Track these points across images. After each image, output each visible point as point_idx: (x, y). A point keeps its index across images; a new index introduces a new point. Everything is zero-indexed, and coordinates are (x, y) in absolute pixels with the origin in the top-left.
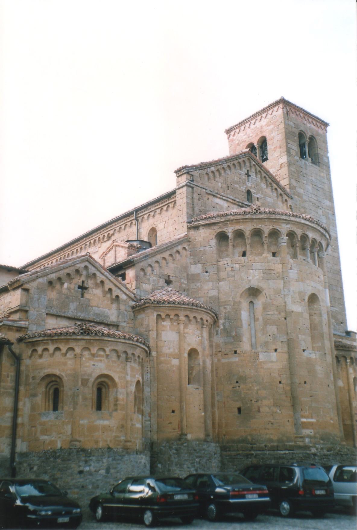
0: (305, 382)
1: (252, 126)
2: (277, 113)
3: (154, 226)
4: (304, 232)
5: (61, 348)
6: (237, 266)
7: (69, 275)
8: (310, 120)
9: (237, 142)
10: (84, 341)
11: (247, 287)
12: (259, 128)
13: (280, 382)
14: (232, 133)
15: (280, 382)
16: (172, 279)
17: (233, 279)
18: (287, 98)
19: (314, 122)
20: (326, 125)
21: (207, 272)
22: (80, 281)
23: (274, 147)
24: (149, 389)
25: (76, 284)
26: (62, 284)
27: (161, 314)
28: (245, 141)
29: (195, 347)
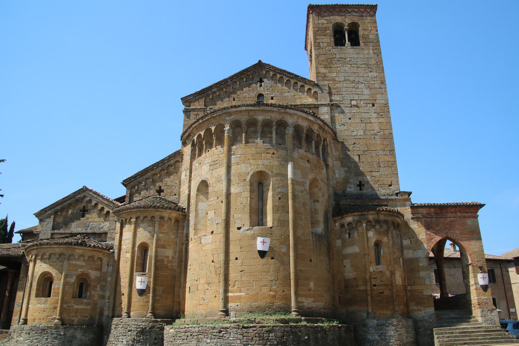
0: (237, 259)
4: (251, 118)
7: (70, 204)
8: (349, 10)
10: (35, 250)
13: (213, 261)
15: (213, 261)
16: (162, 188)
18: (312, 4)
19: (356, 10)
22: (81, 206)
24: (111, 278)
25: (78, 209)
26: (67, 212)
29: (145, 241)
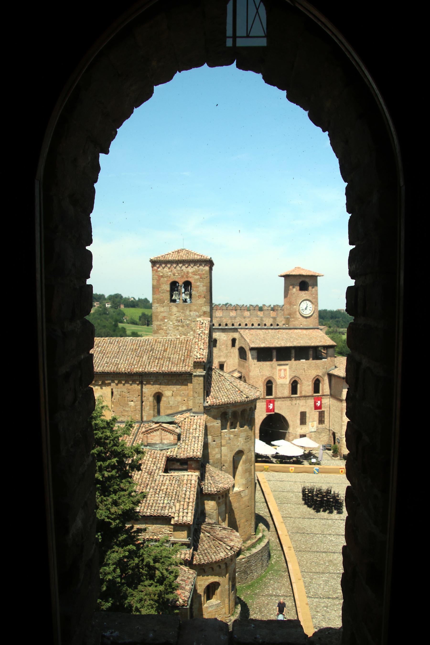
1: (178, 268)
2: (204, 268)
3: (160, 391)
5: (221, 565)
6: (232, 436)
9: (161, 274)
11: (237, 450)
12: (184, 272)
13: (248, 506)
14: (158, 266)
17: (229, 445)
20: (210, 263)
21: (214, 441)
23: (199, 295)
27: (220, 496)
28: (170, 277)
